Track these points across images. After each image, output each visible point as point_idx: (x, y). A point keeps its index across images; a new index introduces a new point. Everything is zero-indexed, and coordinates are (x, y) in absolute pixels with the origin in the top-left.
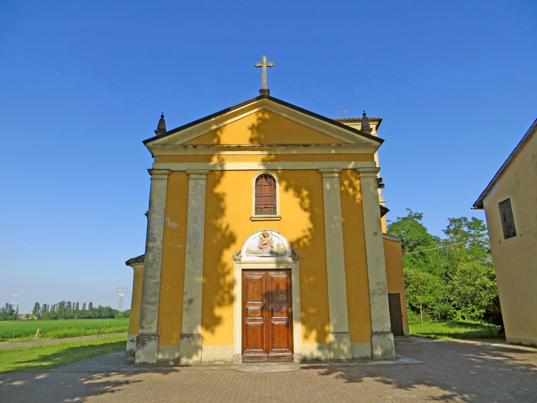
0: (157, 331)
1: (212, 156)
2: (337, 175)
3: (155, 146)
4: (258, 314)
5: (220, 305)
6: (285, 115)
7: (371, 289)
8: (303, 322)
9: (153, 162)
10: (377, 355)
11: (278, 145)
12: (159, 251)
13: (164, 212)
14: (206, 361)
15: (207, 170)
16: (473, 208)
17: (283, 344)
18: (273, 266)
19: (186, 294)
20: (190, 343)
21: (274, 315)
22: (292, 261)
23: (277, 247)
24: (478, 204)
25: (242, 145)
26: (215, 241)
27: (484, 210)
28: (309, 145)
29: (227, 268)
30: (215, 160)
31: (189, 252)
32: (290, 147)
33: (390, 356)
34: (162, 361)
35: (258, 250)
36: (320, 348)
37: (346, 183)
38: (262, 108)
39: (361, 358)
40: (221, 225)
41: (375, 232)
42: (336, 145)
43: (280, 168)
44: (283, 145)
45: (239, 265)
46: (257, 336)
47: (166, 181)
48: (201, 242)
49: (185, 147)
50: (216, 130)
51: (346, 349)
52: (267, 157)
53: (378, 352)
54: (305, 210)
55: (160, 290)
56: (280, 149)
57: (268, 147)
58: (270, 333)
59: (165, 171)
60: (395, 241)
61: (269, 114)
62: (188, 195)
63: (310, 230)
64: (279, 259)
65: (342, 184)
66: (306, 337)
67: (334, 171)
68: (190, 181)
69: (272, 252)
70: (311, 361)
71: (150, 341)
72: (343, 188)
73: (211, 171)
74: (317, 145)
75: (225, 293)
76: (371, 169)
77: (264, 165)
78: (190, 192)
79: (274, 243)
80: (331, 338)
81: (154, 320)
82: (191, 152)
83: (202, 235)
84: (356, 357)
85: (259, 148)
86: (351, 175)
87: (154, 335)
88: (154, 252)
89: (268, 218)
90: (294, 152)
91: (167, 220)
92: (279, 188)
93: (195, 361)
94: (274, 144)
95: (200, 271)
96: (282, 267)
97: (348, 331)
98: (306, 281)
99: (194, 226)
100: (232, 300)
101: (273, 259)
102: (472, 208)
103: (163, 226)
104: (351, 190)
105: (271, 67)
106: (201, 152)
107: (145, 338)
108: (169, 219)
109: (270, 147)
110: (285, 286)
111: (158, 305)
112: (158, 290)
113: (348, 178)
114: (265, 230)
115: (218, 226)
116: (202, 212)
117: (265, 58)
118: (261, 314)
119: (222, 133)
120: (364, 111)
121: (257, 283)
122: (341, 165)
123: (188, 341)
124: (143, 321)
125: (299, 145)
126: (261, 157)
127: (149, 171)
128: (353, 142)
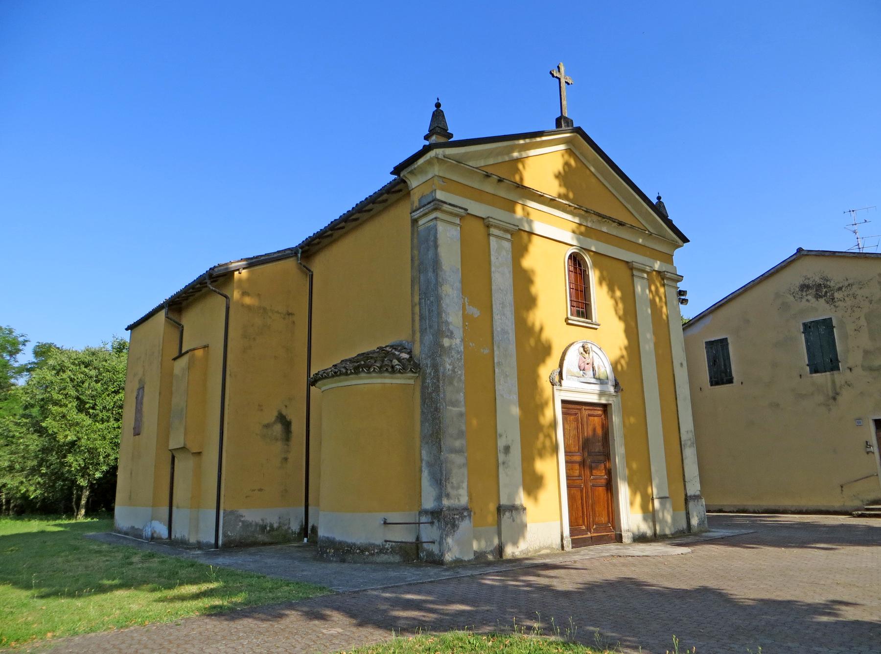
5: (541, 455)
6: (593, 169)
13: (460, 285)
18: (594, 399)
19: (501, 436)
20: (514, 521)
22: (614, 394)
40: (533, 325)
71: (462, 520)
78: (493, 258)
81: (463, 482)
82: (489, 187)
93: (522, 551)
94: (591, 210)
95: (515, 397)
100: (555, 449)
106: (502, 193)
107: (455, 515)
123: (511, 518)
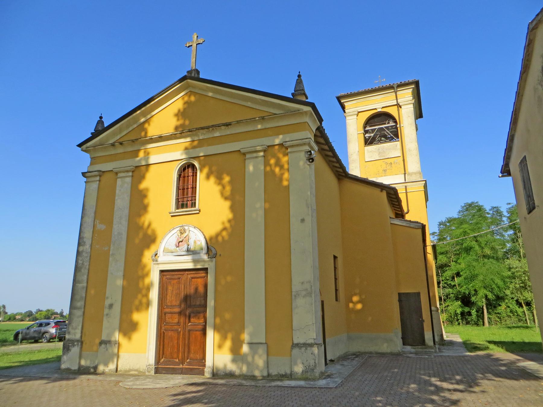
0: (81, 337)
1: (139, 150)
2: (262, 154)
3: (88, 149)
4: (175, 319)
5: (138, 309)
6: (210, 94)
7: (294, 290)
8: (216, 328)
9: (89, 165)
10: (296, 373)
11: (198, 129)
12: (87, 255)
13: (94, 214)
14: (122, 370)
15: (132, 166)
16: (500, 176)
17: (199, 354)
18: (190, 266)
19: (107, 298)
20: (107, 350)
21: (191, 321)
22: (208, 260)
23: (194, 243)
24: (505, 170)
25: (163, 135)
26: (137, 241)
27: (511, 177)
28: (230, 123)
29: (147, 269)
30: (141, 154)
31: (113, 254)
32: (211, 129)
33: (312, 374)
34: (84, 368)
35: (175, 249)
36: (234, 361)
37: (272, 161)
38: (188, 91)
39: (279, 376)
40: (143, 224)
41: (302, 218)
42: (259, 118)
43: (202, 154)
44: (202, 128)
45: (157, 266)
46: (173, 344)
47: (98, 182)
48: (124, 243)
49: (113, 145)
50: (144, 122)
51: (260, 362)
52: (191, 144)
53: (299, 369)
54: (226, 198)
55: (86, 295)
56: (202, 133)
57: (189, 133)
58: (186, 342)
59: (95, 173)
60: (413, 228)
61: (195, 96)
62: (115, 193)
63: (229, 221)
64: (196, 257)
65: (267, 163)
66: (220, 346)
67: (258, 149)
68: (118, 180)
69: (188, 250)
70: (223, 375)
71: (74, 347)
72: (268, 169)
73: (137, 167)
74: (238, 122)
75: (143, 296)
76: (300, 141)
77: (186, 153)
78: (117, 192)
79: (191, 240)
80: (245, 349)
81: (79, 326)
82: (120, 150)
83: (124, 236)
84: (273, 374)
85: (181, 135)
86: (279, 151)
87: (78, 341)
88: (83, 256)
89: (186, 211)
90: (217, 134)
91: (96, 223)
92: (201, 176)
93: (111, 369)
94: (193, 129)
95: (121, 274)
96: (199, 267)
97: (264, 342)
98: (223, 282)
99: (118, 227)
100: (148, 304)
101: (189, 258)
102: (499, 177)
103: (92, 229)
104: (277, 170)
105: (202, 44)
106: (130, 149)
107: (69, 344)
108: (98, 221)
109: (190, 133)
110: (203, 289)
111: (83, 310)
112: (84, 295)
113: (274, 156)
114: (182, 225)
115: (141, 224)
116: (126, 212)
117: (195, 36)
118: (179, 320)
119: (149, 125)
120: (299, 72)
121: (176, 285)
122: (267, 141)
123: (106, 348)
124: (69, 326)
125: (219, 126)
126: (183, 146)
127: (84, 174)
128: (282, 112)
